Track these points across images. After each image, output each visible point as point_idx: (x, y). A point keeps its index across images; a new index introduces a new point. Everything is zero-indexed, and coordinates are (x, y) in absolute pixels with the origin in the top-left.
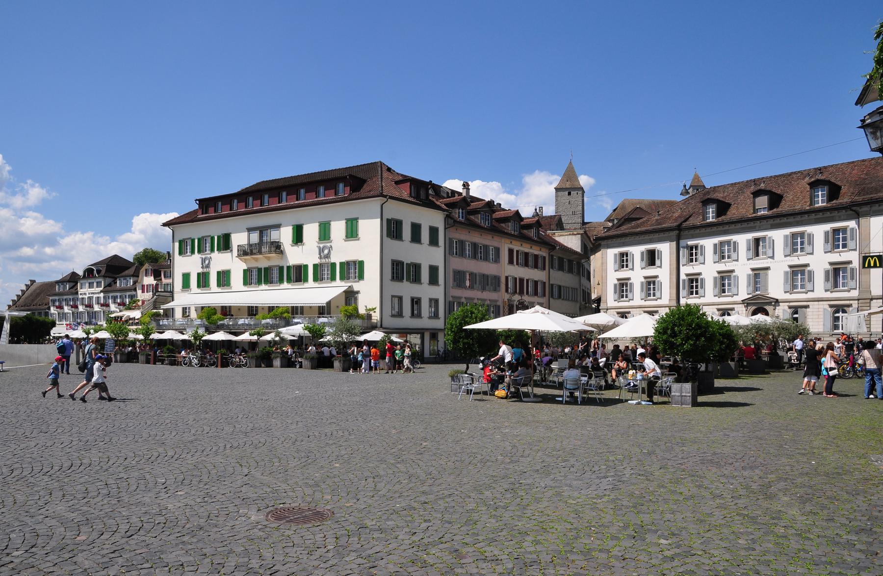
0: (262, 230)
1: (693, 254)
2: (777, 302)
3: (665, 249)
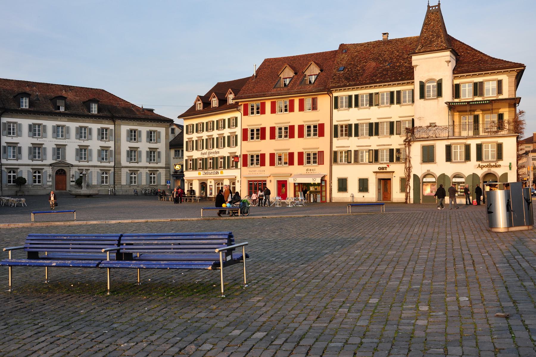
2: (72, 166)
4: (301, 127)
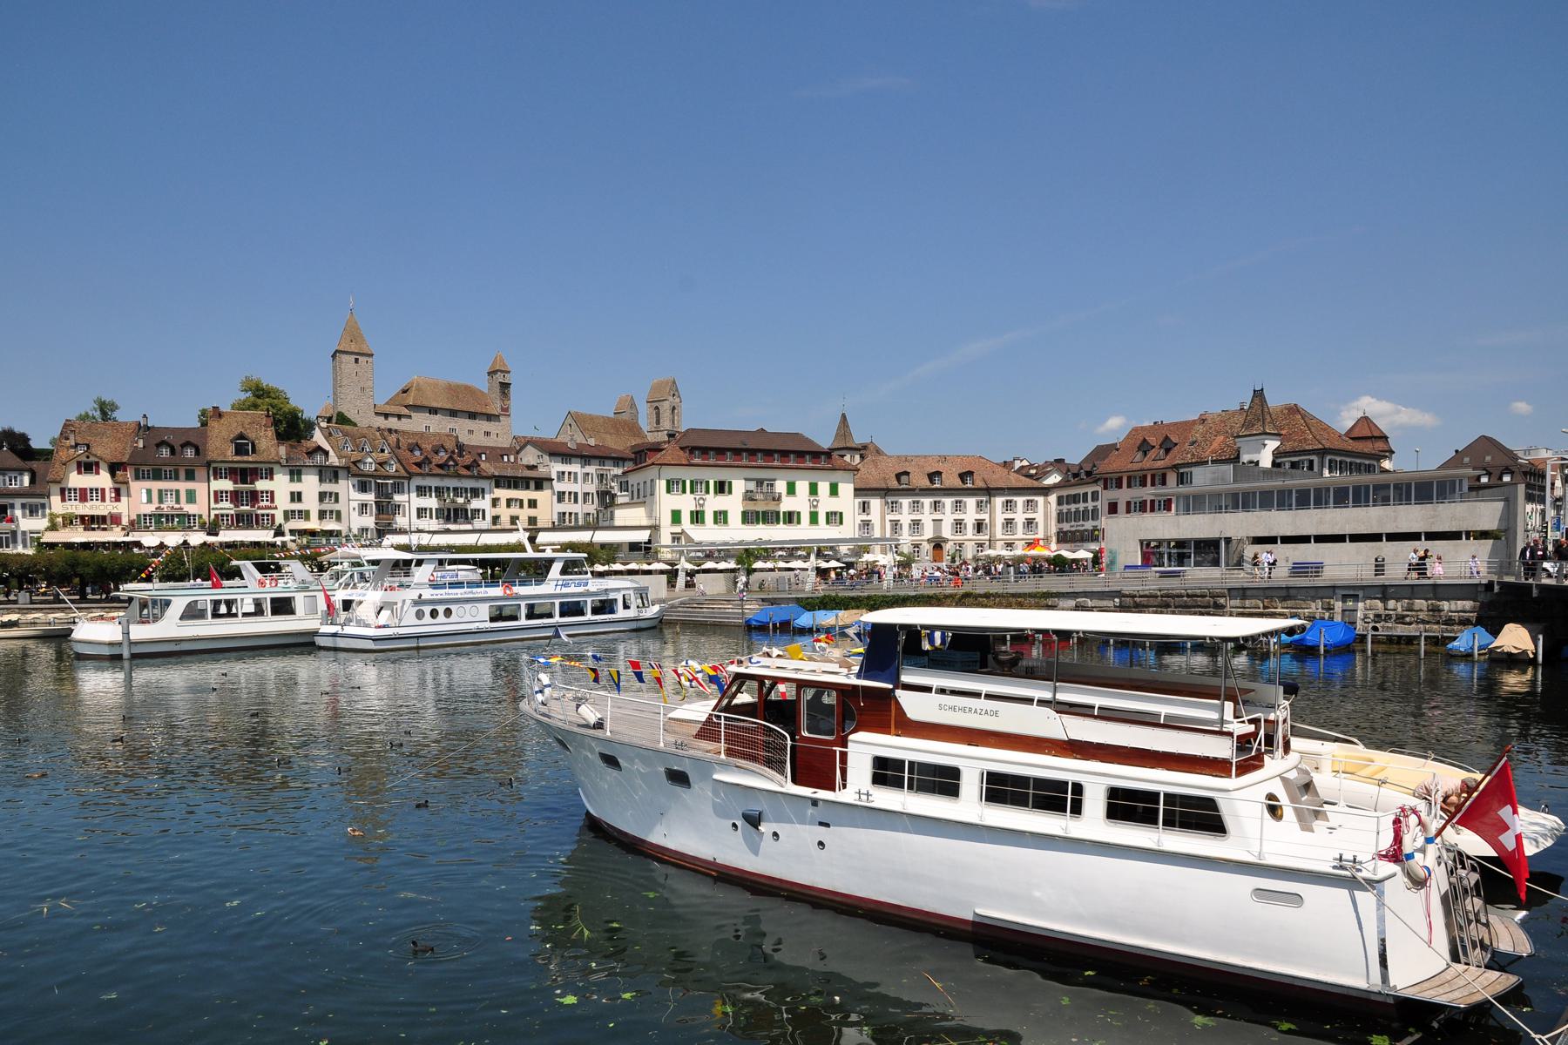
0: (760, 483)
1: (894, 507)
3: (876, 503)
4: (1152, 502)
